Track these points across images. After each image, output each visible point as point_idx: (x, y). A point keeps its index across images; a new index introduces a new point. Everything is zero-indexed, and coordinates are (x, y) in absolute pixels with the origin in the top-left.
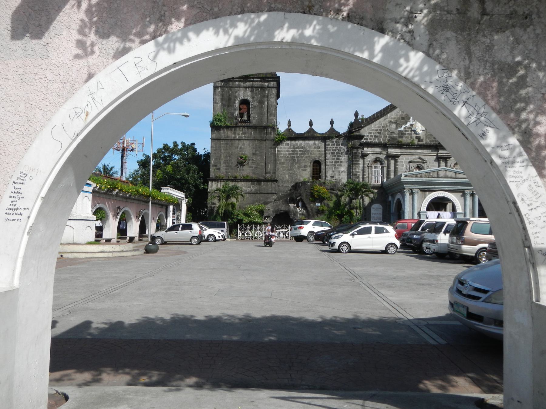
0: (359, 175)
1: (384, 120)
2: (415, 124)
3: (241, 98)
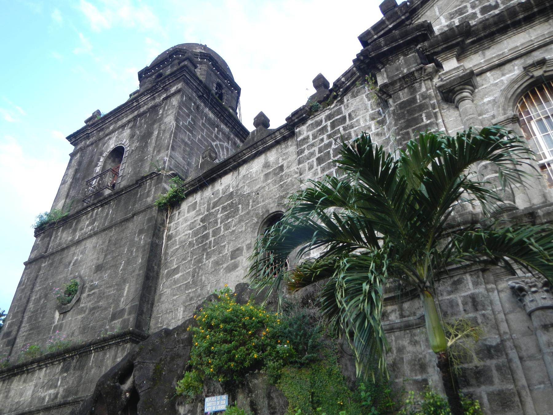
3: (108, 151)
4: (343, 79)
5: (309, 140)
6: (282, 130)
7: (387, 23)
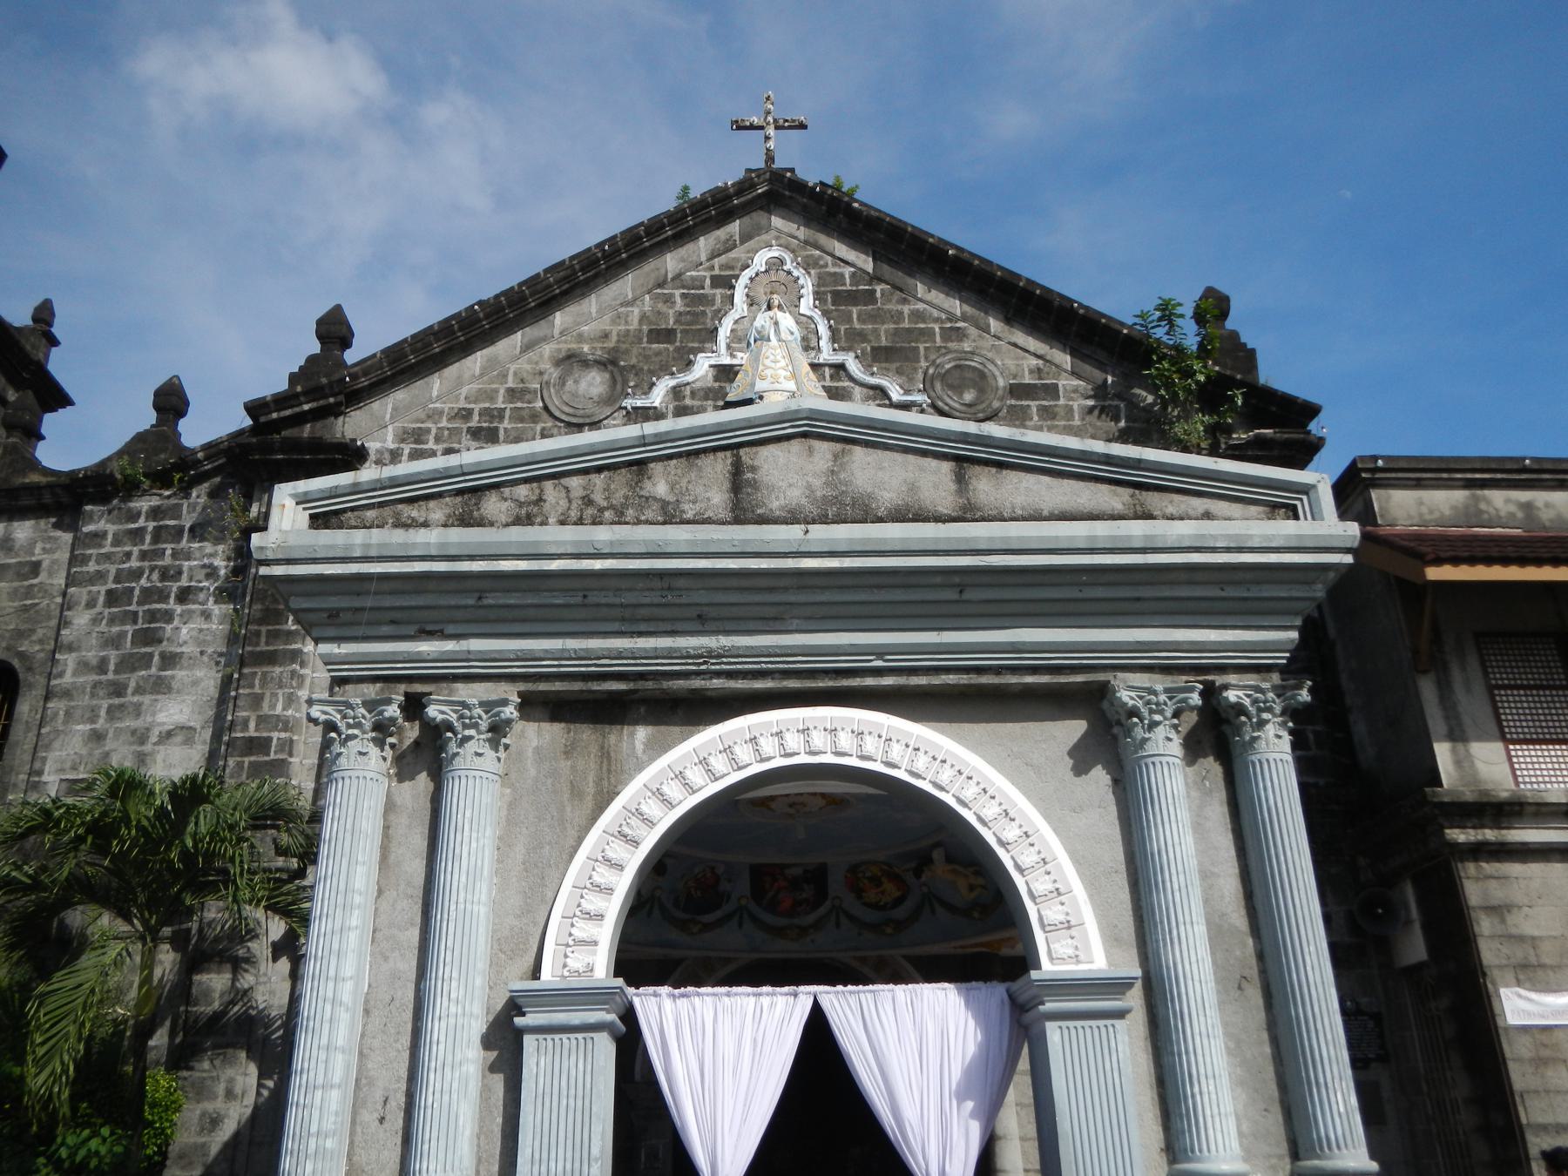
0: (288, 746)
1: (527, 347)
2: (747, 367)
4: (200, 455)
5: (104, 542)
6: (59, 491)
7: (302, 399)
